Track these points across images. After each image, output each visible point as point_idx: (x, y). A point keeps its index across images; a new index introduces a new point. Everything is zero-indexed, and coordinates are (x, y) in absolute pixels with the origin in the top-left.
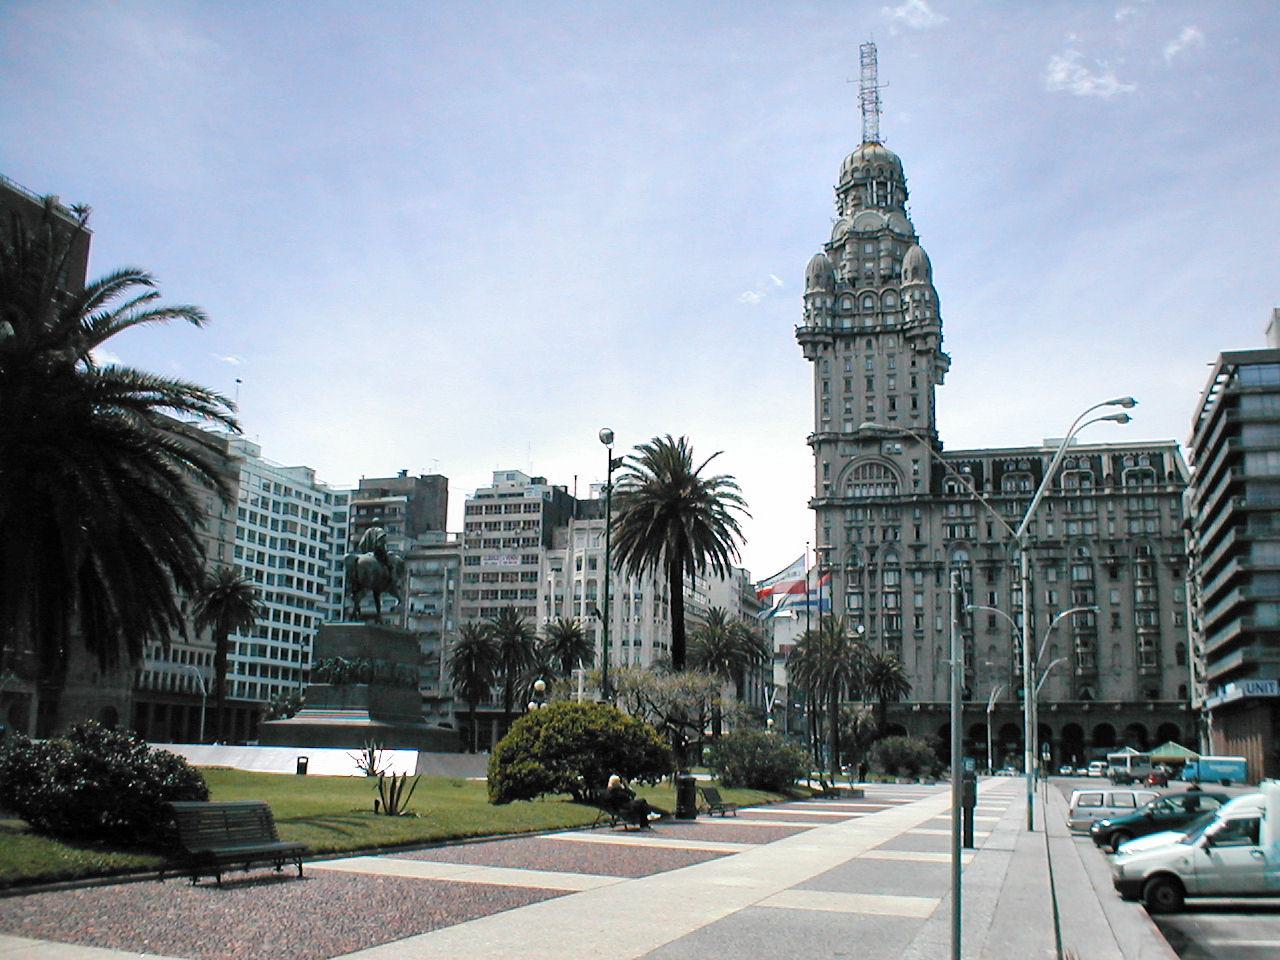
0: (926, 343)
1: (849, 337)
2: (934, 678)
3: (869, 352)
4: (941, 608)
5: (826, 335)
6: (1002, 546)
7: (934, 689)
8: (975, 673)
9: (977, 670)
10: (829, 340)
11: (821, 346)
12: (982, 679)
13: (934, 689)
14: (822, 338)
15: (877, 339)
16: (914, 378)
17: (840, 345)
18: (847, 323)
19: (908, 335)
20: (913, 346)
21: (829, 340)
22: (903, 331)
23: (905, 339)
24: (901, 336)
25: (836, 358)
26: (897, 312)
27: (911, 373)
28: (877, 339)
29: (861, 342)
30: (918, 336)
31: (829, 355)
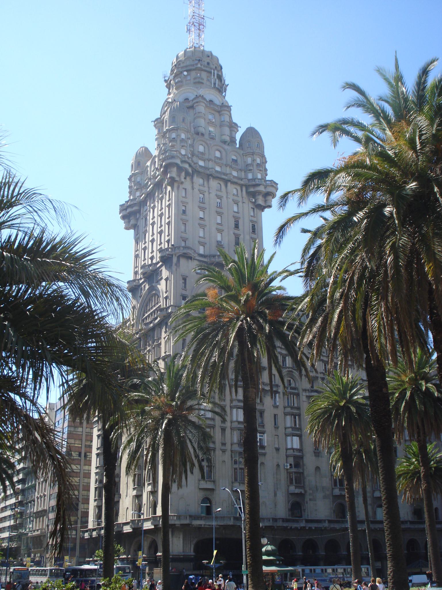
0: (266, 201)
1: (208, 176)
2: (275, 495)
3: (219, 193)
4: (278, 428)
5: (190, 166)
6: (319, 379)
7: (275, 505)
8: (306, 492)
9: (307, 489)
10: (190, 170)
11: (183, 174)
12: (311, 497)
13: (275, 505)
14: (186, 166)
15: (226, 186)
16: (253, 227)
17: (198, 181)
18: (201, 163)
19: (252, 190)
20: (254, 201)
21: (190, 170)
22: (247, 187)
23: (248, 193)
24: (244, 189)
25: (193, 188)
26: (241, 170)
27: (251, 221)
28: (226, 186)
29: (214, 184)
30: (259, 193)
31: (187, 184)
